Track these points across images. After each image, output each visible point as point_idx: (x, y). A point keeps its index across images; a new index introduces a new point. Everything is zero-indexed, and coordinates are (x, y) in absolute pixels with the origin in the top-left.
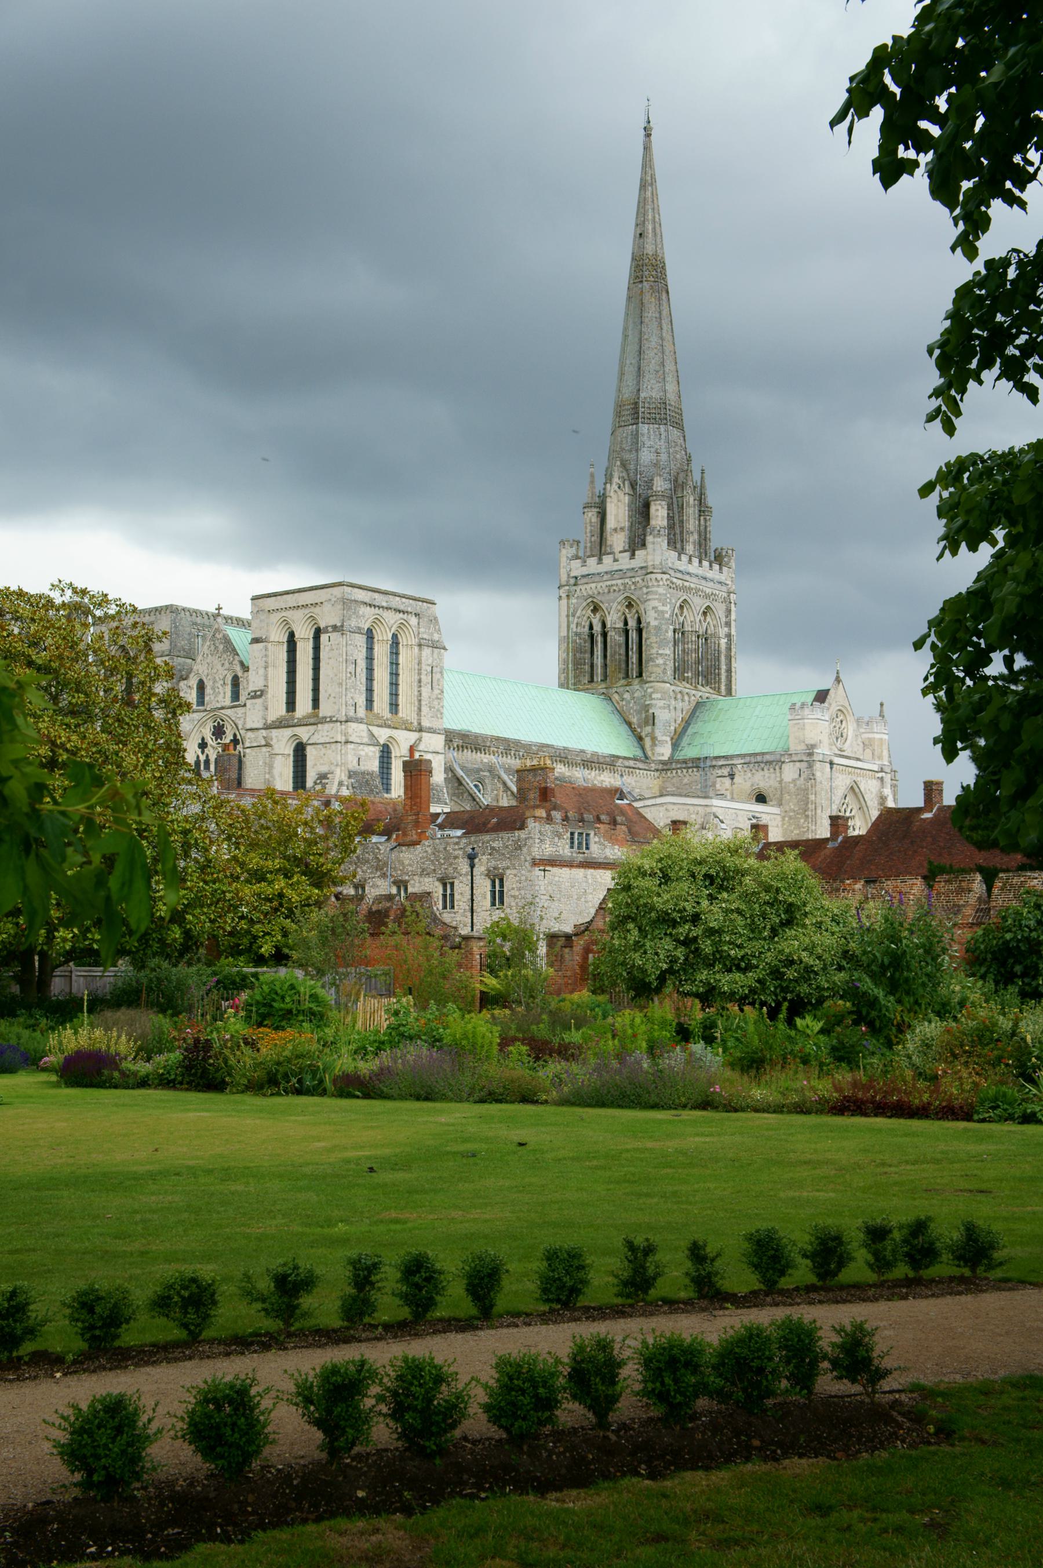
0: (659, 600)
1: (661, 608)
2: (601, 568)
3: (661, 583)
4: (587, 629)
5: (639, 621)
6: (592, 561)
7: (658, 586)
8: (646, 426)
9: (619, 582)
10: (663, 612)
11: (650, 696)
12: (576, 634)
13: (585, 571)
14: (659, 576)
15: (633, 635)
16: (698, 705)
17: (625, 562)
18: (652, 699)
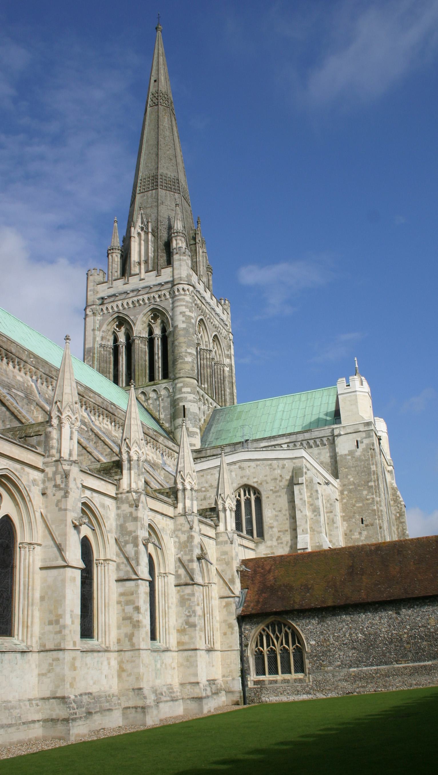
0: (187, 307)
1: (188, 313)
2: (128, 288)
3: (187, 292)
4: (111, 343)
5: (164, 330)
6: (119, 286)
7: (185, 295)
8: (164, 192)
9: (146, 297)
10: (190, 317)
11: (180, 390)
12: (101, 346)
13: (111, 292)
14: (186, 287)
15: (158, 343)
16: (215, 411)
17: (151, 279)
18: (182, 393)
